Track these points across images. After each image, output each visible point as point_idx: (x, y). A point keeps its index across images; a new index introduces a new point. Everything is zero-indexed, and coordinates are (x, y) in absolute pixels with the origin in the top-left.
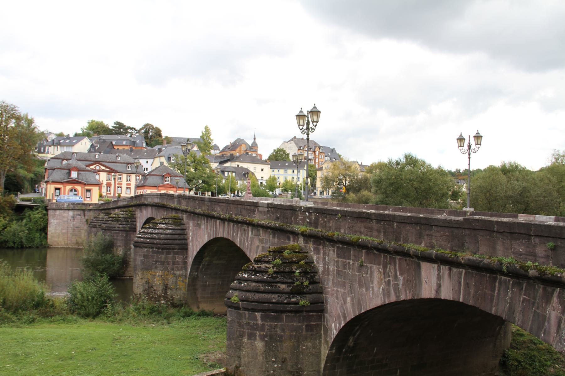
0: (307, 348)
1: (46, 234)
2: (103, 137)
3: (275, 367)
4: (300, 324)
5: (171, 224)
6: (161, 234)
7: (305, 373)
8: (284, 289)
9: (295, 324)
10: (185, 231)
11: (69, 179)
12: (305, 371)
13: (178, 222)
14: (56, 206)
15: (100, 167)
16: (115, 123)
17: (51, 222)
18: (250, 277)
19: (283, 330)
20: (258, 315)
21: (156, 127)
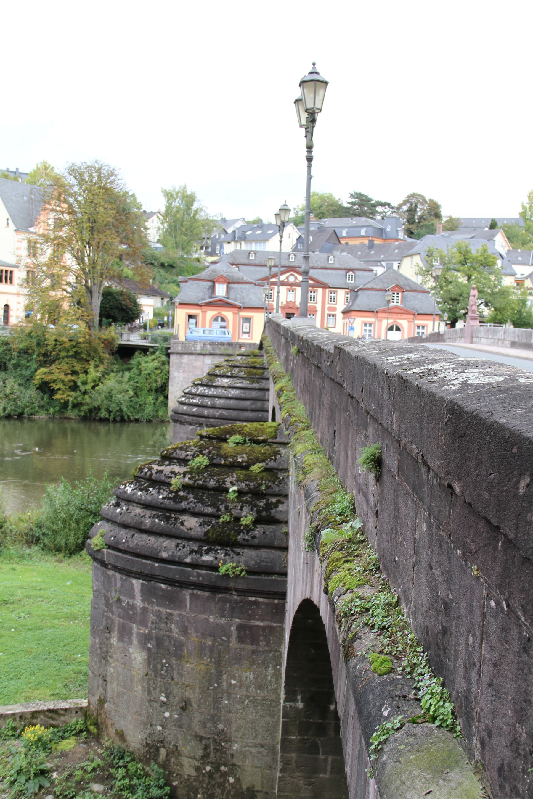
0: (241, 684)
1: (166, 397)
2: (325, 222)
3: (166, 719)
4: (223, 621)
5: (242, 378)
6: (219, 397)
7: (235, 747)
8: (191, 529)
9: (212, 619)
10: (267, 393)
11: (211, 297)
12: (237, 742)
13: (255, 374)
14: (182, 347)
15: (296, 278)
16: (352, 196)
17: (175, 377)
18: (135, 494)
19: (185, 631)
20: (137, 583)
21: (430, 200)
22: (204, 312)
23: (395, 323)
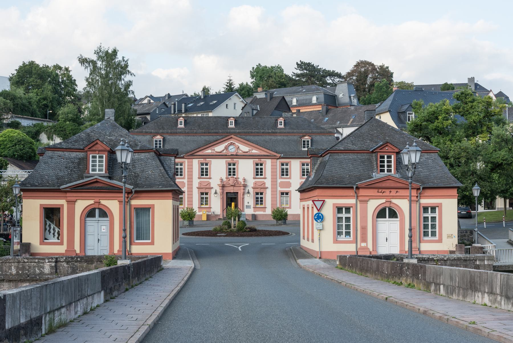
22: (72, 203)
23: (388, 205)
